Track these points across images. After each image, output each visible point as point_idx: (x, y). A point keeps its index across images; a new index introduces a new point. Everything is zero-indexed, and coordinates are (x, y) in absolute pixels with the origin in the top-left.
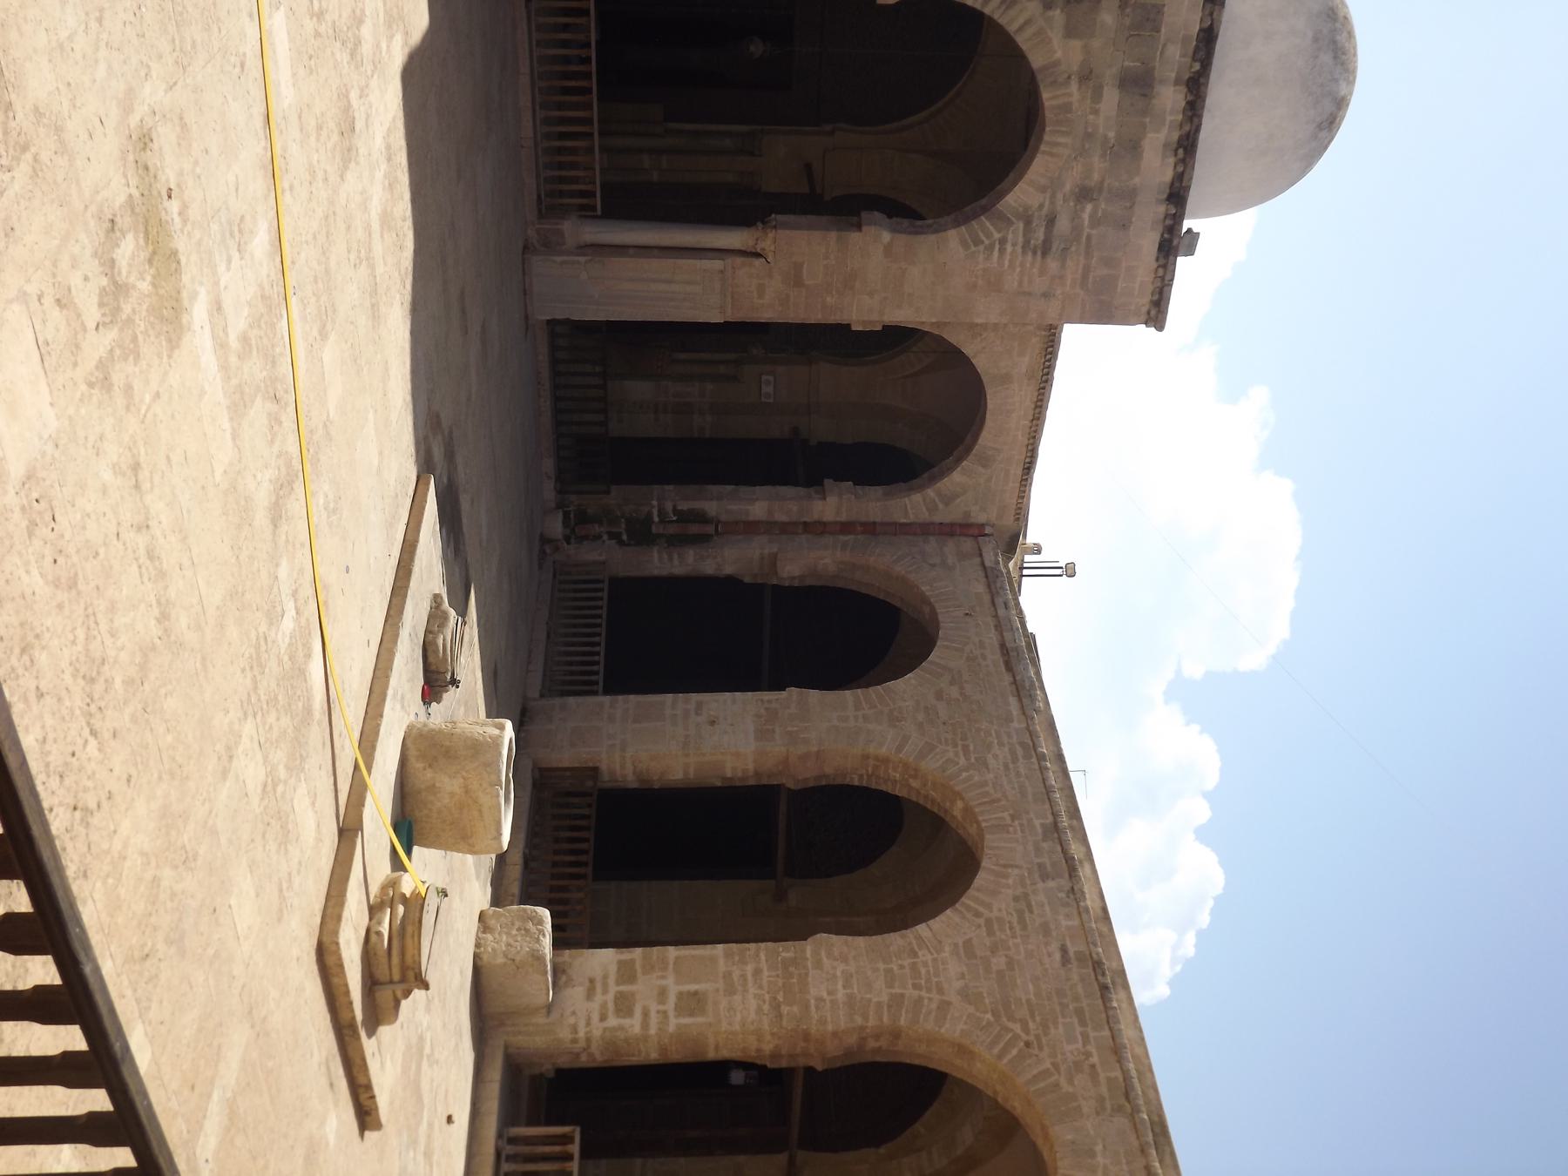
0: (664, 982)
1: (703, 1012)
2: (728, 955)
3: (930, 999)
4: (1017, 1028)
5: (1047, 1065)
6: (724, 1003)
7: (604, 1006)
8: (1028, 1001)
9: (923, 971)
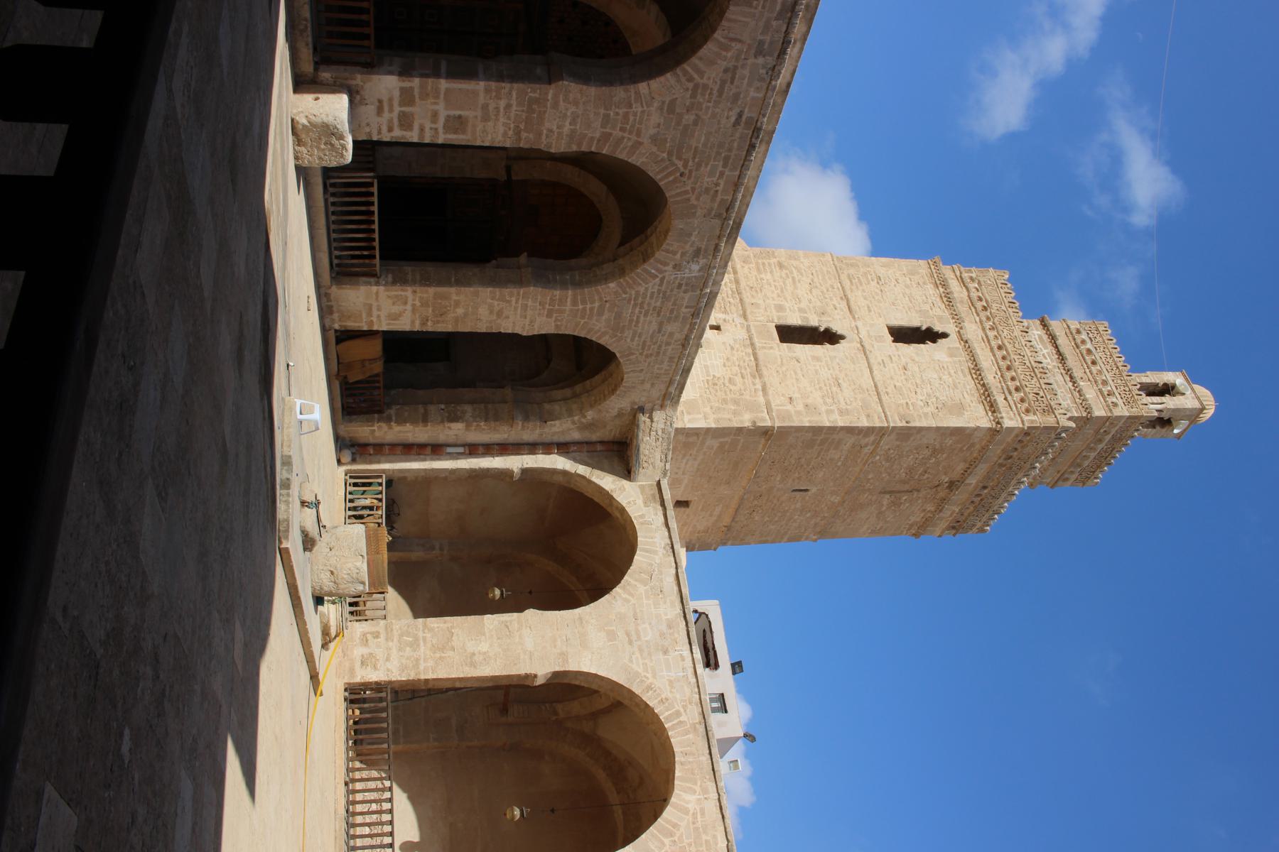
0: (436, 107)
1: (464, 132)
2: (487, 91)
4: (680, 164)
5: (689, 188)
6: (480, 127)
7: (391, 121)
9: (632, 118)
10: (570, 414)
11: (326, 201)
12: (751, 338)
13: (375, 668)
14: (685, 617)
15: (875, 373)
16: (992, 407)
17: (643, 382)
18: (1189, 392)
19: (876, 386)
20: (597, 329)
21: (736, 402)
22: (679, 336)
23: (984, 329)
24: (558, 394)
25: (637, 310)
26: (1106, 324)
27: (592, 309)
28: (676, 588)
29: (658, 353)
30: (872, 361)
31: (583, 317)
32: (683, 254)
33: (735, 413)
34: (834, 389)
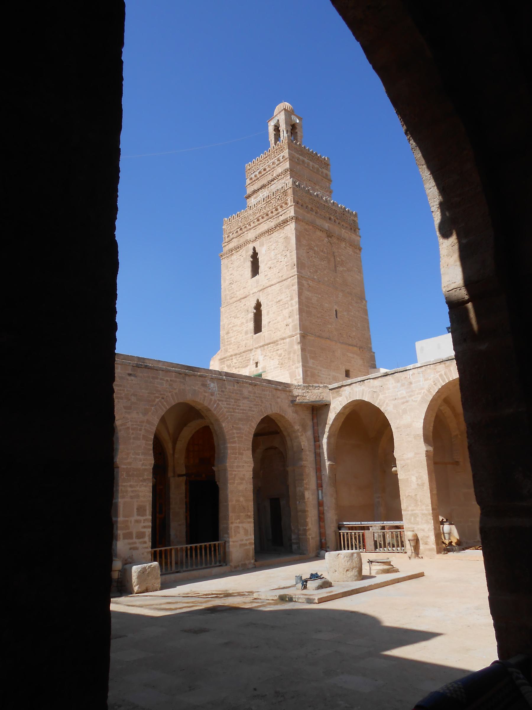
2: (123, 497)
3: (145, 426)
4: (157, 400)
5: (170, 394)
7: (140, 543)
8: (148, 393)
9: (135, 426)
10: (297, 437)
11: (184, 571)
12: (261, 347)
13: (428, 537)
14: (393, 374)
15: (273, 283)
16: (285, 222)
17: (277, 403)
18: (277, 118)
19: (279, 282)
20: (249, 429)
21: (289, 353)
22: (250, 389)
23: (250, 229)
24: (289, 443)
25: (237, 411)
26: (246, 165)
27: (237, 433)
28: (380, 379)
29: (260, 397)
30: (268, 285)
31: (242, 437)
32: (205, 392)
33: (294, 353)
34: (281, 303)
